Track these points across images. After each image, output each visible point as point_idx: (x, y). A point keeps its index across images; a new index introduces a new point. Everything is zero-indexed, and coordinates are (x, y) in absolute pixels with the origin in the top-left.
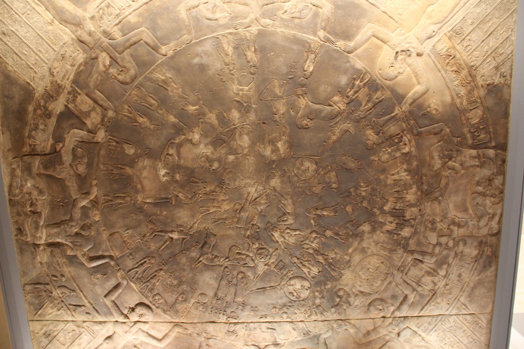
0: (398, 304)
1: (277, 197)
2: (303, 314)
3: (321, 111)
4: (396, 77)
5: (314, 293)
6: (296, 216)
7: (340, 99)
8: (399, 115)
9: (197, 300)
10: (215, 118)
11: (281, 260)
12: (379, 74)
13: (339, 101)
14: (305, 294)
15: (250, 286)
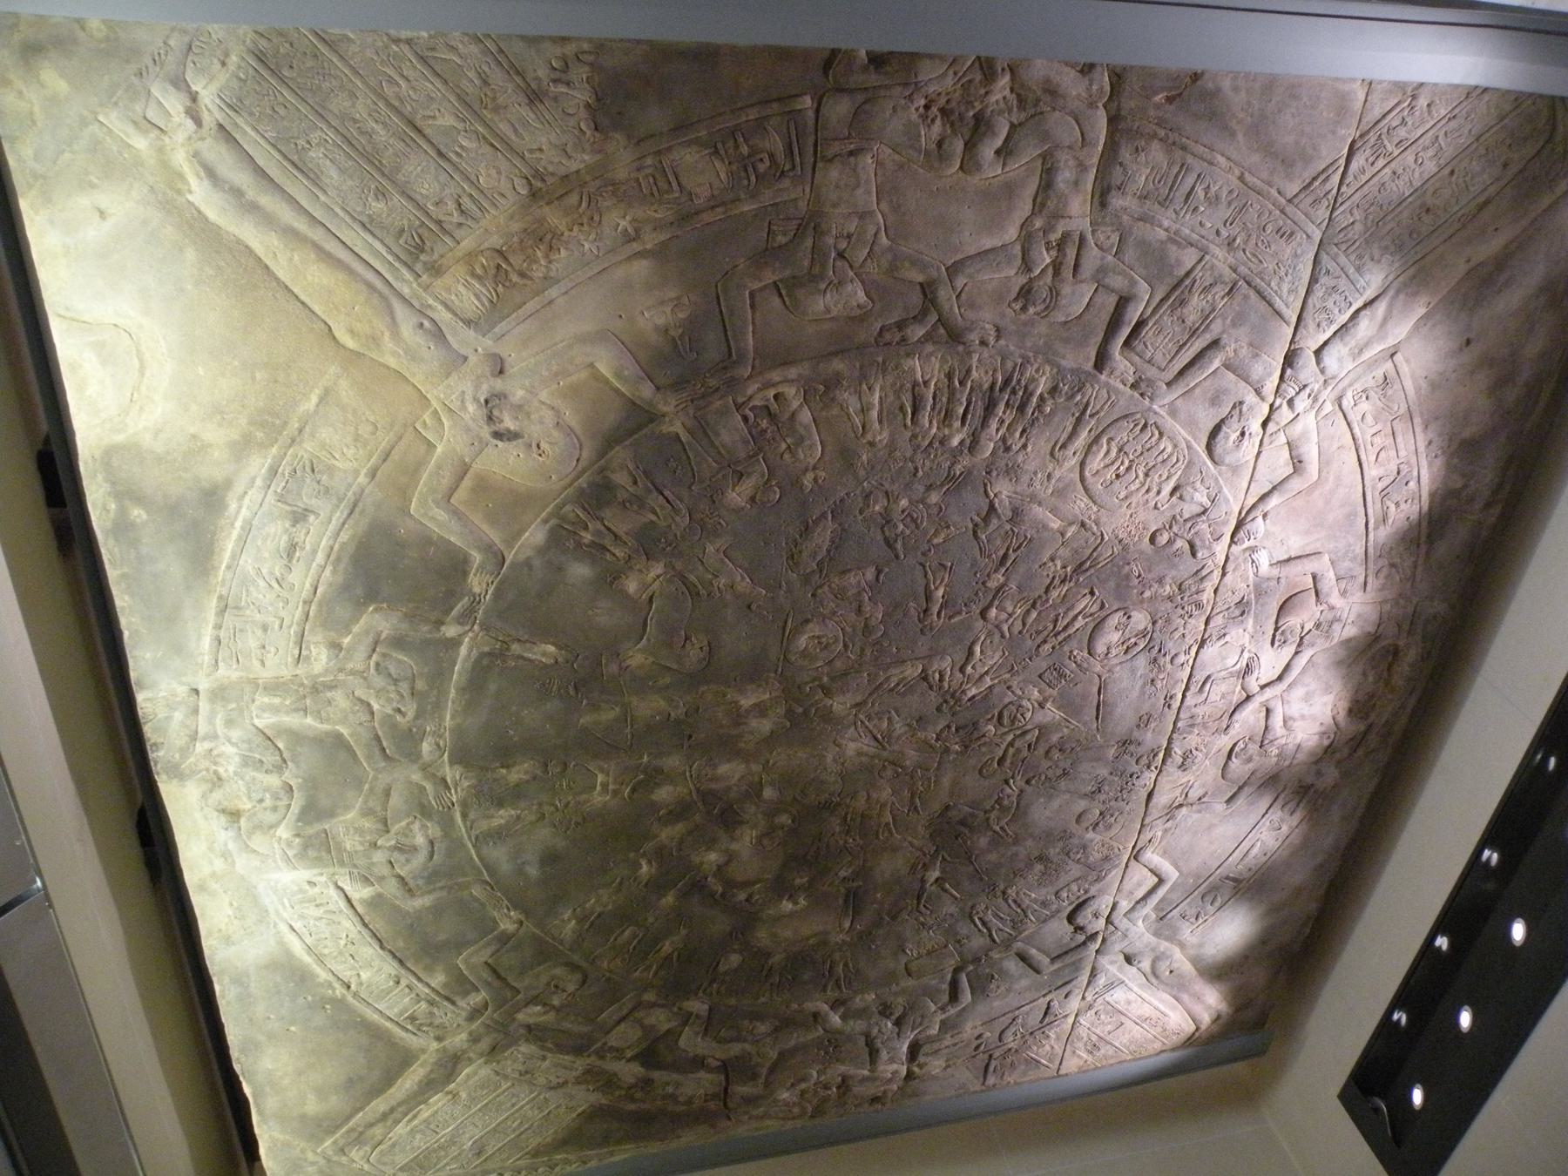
11: (1040, 676)
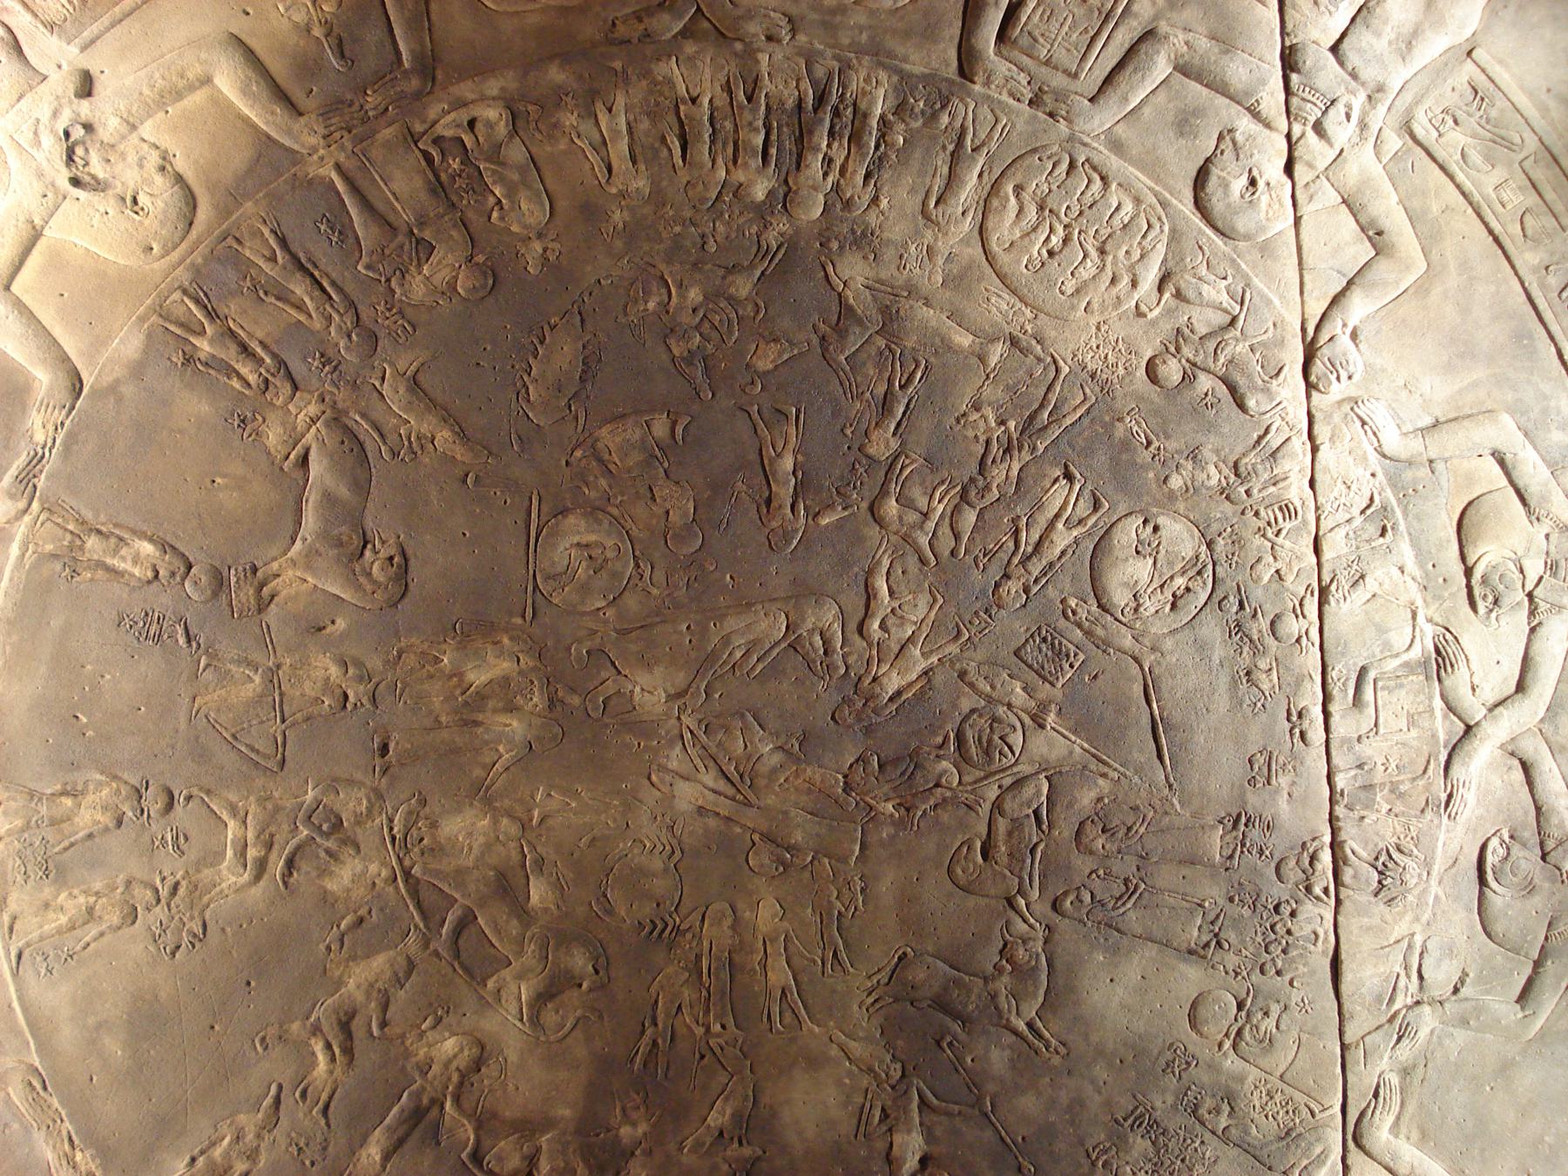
0: (1222, 101)
1: (718, 685)
2: (1280, 540)
3: (328, 498)
4: (179, 179)
5: (1171, 497)
6: (804, 592)
7: (272, 417)
8: (342, 159)
9: (1228, 1044)
10: (363, 963)
12: (166, 253)
13: (283, 424)
14: (1179, 536)
15: (1143, 794)
